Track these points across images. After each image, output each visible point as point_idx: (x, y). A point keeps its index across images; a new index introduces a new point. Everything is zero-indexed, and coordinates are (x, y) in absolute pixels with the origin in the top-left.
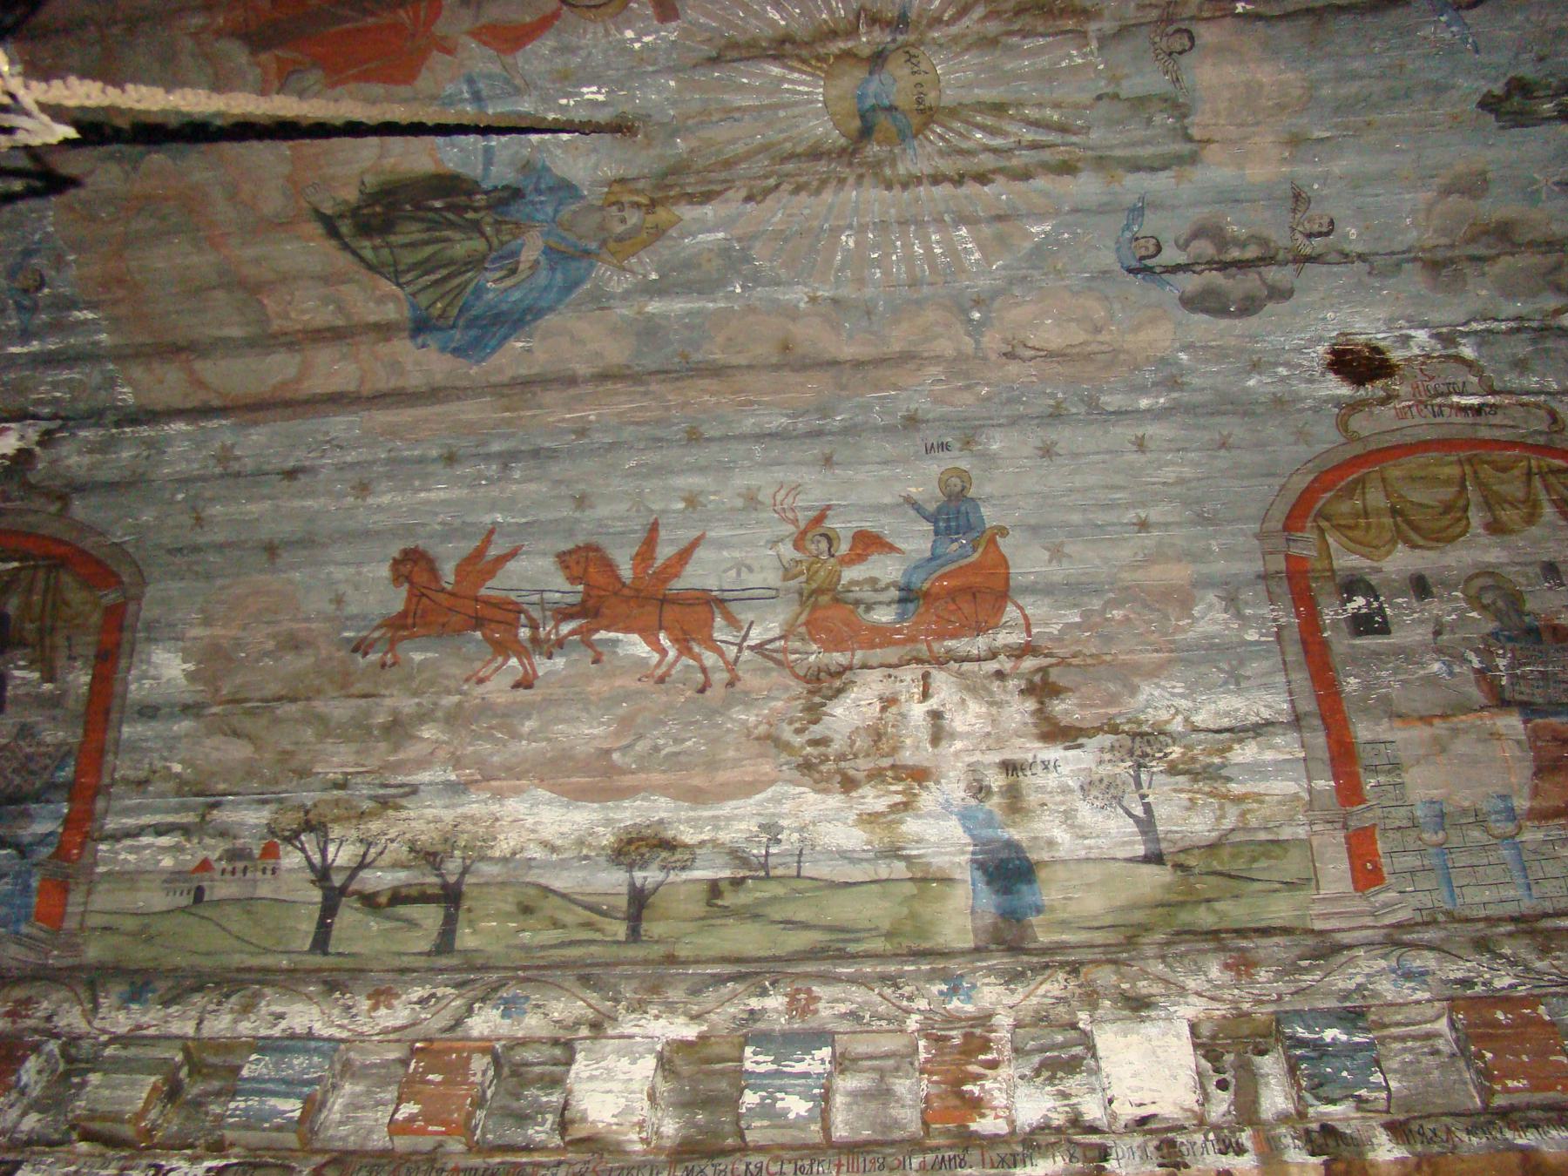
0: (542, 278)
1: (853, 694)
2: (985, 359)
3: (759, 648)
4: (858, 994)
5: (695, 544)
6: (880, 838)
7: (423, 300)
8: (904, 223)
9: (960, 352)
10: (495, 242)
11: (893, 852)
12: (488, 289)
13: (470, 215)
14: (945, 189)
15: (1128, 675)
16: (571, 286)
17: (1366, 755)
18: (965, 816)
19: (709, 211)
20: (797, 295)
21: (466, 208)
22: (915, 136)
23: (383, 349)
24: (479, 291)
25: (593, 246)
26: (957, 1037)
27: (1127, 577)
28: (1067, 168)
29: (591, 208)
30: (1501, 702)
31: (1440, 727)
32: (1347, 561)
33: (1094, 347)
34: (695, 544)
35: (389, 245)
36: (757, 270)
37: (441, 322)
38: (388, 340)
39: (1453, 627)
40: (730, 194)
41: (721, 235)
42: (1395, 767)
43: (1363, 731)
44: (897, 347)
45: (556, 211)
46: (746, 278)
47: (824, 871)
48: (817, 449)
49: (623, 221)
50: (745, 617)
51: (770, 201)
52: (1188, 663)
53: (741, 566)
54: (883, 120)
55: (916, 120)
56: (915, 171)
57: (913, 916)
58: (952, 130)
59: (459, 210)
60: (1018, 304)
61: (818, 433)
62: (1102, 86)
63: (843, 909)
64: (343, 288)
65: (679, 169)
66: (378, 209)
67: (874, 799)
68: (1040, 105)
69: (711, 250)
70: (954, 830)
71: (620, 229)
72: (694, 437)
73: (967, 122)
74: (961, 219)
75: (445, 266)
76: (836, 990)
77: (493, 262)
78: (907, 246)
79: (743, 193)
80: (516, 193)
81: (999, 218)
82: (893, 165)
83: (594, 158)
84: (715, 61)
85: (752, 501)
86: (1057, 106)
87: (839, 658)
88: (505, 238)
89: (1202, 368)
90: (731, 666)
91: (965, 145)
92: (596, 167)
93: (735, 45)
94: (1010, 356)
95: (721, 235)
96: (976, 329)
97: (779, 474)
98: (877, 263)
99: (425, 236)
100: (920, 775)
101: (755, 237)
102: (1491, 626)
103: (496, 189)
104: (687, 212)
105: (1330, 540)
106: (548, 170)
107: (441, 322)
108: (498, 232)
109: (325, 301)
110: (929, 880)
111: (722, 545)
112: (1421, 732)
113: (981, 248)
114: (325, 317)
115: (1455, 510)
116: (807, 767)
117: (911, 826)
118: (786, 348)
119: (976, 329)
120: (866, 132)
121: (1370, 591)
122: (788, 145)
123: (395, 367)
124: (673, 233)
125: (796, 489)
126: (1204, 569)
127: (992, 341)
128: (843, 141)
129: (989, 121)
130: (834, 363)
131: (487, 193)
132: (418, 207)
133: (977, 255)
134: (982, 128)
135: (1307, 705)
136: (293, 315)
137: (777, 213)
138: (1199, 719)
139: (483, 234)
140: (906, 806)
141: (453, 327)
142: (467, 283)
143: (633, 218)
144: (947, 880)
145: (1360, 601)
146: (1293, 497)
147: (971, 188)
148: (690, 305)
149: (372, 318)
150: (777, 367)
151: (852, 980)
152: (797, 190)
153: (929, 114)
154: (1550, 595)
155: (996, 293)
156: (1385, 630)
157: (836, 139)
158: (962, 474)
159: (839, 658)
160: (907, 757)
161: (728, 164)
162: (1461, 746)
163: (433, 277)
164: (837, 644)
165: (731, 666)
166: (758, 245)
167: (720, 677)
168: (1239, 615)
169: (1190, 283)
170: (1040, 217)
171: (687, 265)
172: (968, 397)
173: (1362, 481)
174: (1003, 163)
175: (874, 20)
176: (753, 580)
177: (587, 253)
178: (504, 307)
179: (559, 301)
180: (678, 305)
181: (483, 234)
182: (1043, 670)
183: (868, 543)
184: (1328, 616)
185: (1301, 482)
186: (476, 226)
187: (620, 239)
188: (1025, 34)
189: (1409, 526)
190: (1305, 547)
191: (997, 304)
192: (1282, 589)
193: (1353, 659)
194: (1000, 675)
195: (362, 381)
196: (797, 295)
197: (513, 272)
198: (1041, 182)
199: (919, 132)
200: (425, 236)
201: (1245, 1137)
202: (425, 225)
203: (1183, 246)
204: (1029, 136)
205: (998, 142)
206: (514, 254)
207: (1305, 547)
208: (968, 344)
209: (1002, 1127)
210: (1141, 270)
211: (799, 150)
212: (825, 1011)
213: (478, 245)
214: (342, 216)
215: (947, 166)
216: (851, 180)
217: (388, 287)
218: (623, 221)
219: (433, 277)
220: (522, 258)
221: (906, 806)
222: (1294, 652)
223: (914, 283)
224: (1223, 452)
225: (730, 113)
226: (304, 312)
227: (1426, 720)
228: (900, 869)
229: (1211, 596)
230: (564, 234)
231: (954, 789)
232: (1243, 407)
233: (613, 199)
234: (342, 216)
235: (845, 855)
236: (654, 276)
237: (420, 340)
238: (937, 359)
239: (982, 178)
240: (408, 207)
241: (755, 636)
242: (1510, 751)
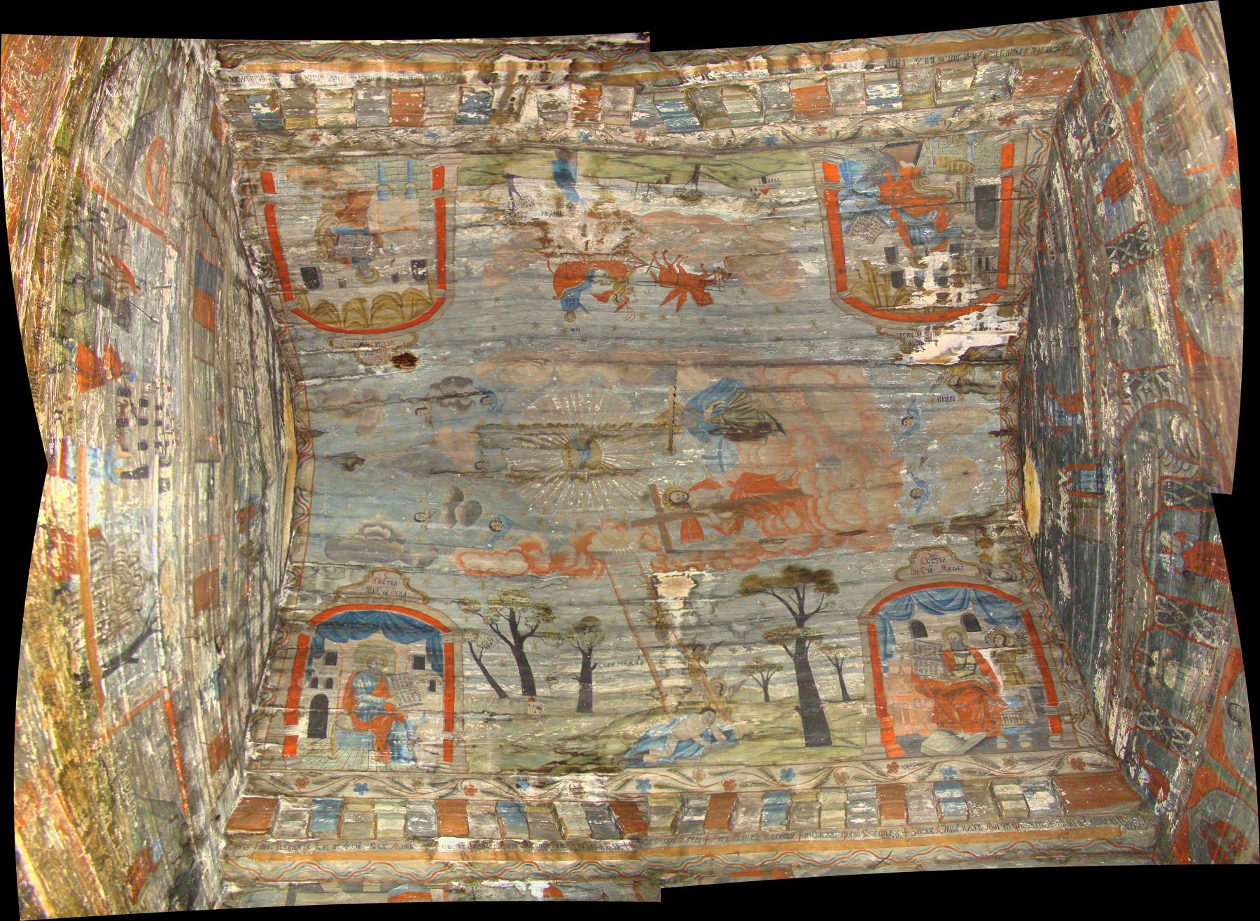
0: (705, 402)
8: (578, 412)
14: (563, 422)
16: (695, 399)
19: (645, 421)
24: (727, 400)
28: (522, 427)
30: (375, 236)
53: (648, 294)
54: (582, 446)
62: (507, 452)
65: (654, 436)
74: (558, 412)
80: (711, 433)
84: (638, 470)
93: (631, 475)
96: (555, 374)
101: (630, 411)
104: (652, 421)
119: (555, 374)
120: (588, 443)
126: (477, 284)
137: (622, 419)
145: (420, 273)
153: (567, 447)
156: (413, 262)
157: (599, 442)
161: (636, 436)
171: (653, 403)
175: (582, 479)
184: (434, 267)
186: (727, 422)
188: (532, 471)
192: (448, 277)
198: (530, 423)
204: (533, 438)
213: (727, 417)
215: (563, 430)
225: (634, 452)
239: (550, 425)
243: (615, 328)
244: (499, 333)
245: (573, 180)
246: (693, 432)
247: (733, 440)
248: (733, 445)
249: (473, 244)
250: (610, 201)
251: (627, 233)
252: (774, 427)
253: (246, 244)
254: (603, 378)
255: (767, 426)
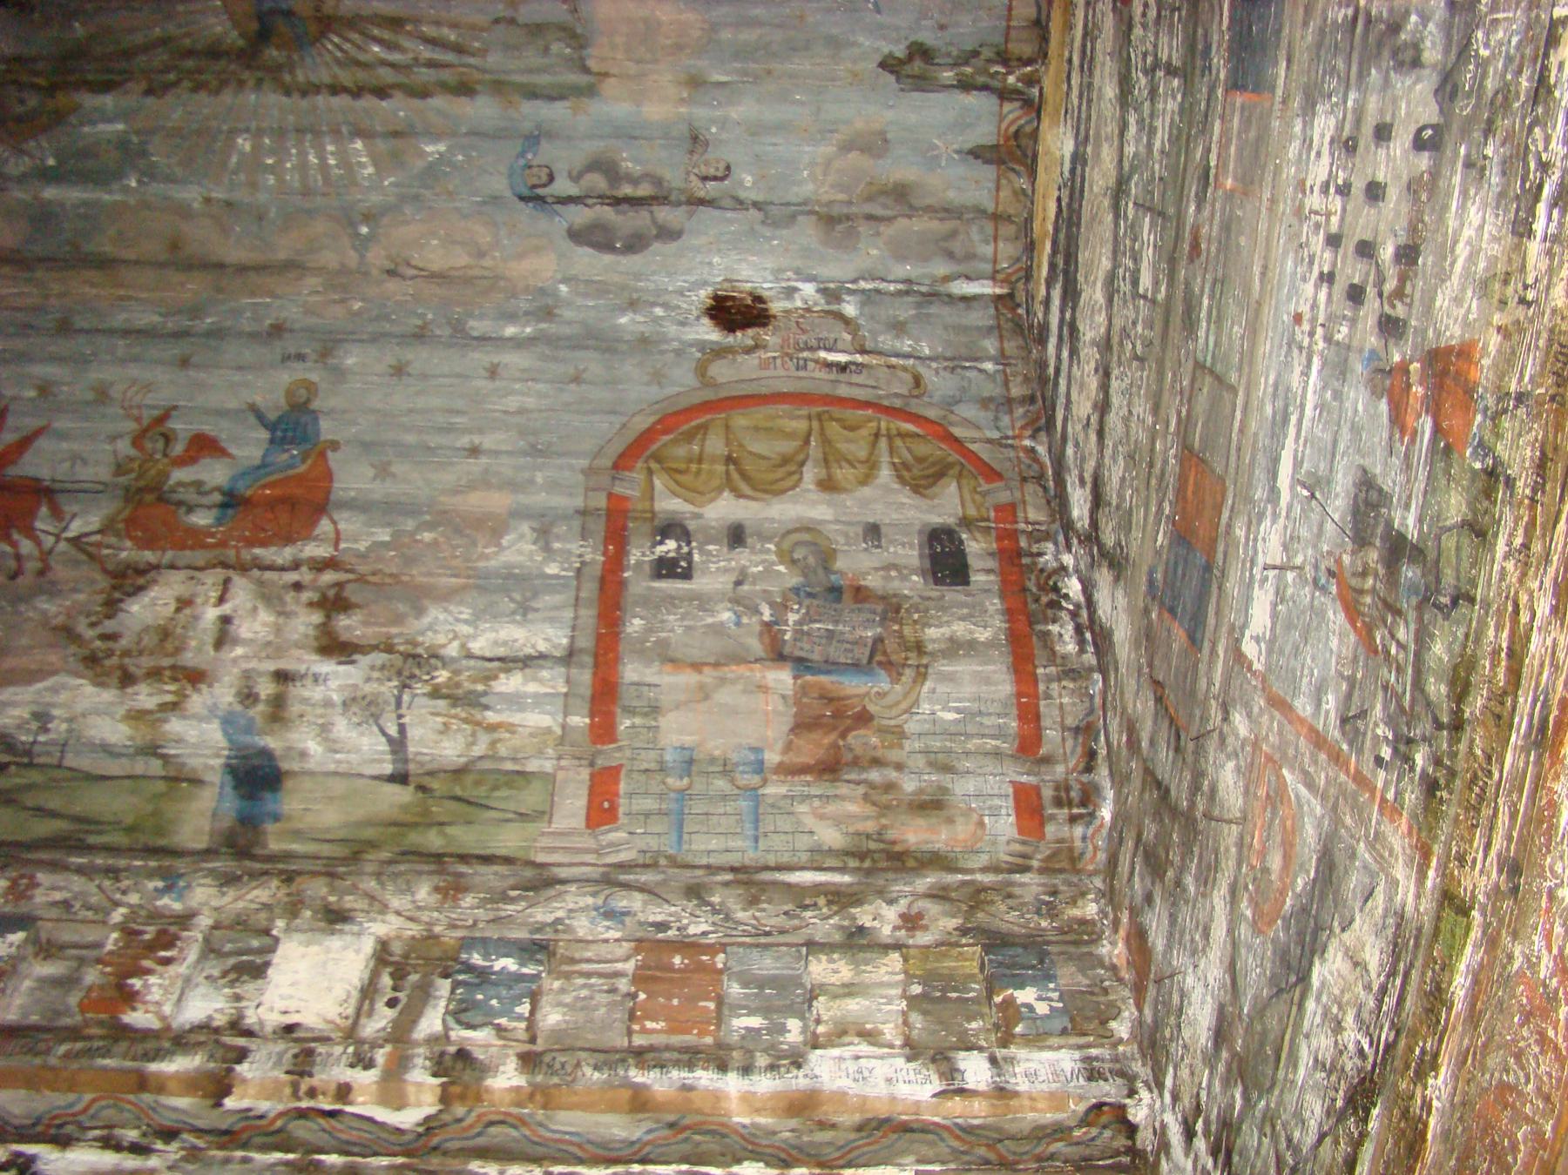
1: (154, 592)
2: (366, 274)
3: (76, 541)
4: (78, 883)
5: (39, 432)
6: (143, 735)
8: (300, 131)
9: (343, 265)
11: (152, 750)
14: (343, 101)
15: (419, 598)
17: (627, 696)
18: (228, 721)
19: (108, 101)
20: (191, 194)
22: (312, 44)
26: (150, 933)
27: (447, 501)
28: (464, 89)
30: (778, 655)
31: (709, 675)
32: (670, 504)
33: (477, 272)
34: (39, 432)
36: (153, 165)
39: (756, 578)
41: (120, 127)
42: (654, 710)
43: (631, 671)
44: (282, 255)
47: (85, 763)
48: (175, 350)
49: (22, 102)
50: (69, 509)
51: (169, 98)
52: (482, 589)
54: (281, 25)
55: (313, 28)
56: (314, 79)
57: (156, 813)
58: (347, 40)
60: (407, 223)
61: (179, 335)
63: (97, 802)
67: (146, 697)
68: (438, 23)
70: (213, 733)
72: (65, 328)
73: (362, 33)
74: (358, 133)
76: (58, 879)
78: (303, 154)
79: (144, 85)
81: (396, 134)
82: (292, 72)
85: (102, 395)
86: (454, 26)
87: (149, 556)
89: (580, 301)
90: (45, 555)
91: (362, 57)
94: (391, 273)
95: (120, 127)
97: (134, 371)
98: (271, 169)
100: (196, 677)
101: (152, 132)
102: (795, 580)
104: (89, 101)
105: (657, 483)
110: (181, 779)
111: (63, 436)
112: (688, 678)
113: (376, 165)
115: (791, 465)
116: (92, 660)
117: (175, 726)
118: (175, 246)
119: (362, 244)
120: (264, 35)
121: (685, 535)
122: (187, 42)
124: (73, 120)
125: (148, 387)
126: (523, 499)
127: (377, 257)
128: (241, 43)
129: (386, 35)
130: (221, 266)
133: (370, 170)
134: (380, 41)
135: (586, 642)
138: (476, 646)
140: (174, 706)
143: (33, 101)
144: (196, 782)
145: (671, 545)
146: (631, 436)
147: (368, 102)
150: (162, 265)
151: (80, 870)
152: (196, 89)
154: (862, 556)
155: (386, 210)
156: (687, 575)
157: (234, 38)
158: (311, 388)
159: (149, 556)
160: (189, 658)
161: (128, 54)
162: (724, 696)
164: (148, 543)
165: (45, 555)
166: (157, 139)
167: (32, 566)
168: (547, 549)
169: (580, 216)
170: (436, 137)
171: (85, 154)
172: (339, 311)
173: (704, 428)
174: (402, 79)
176: (86, 473)
180: (73, 195)
182: (340, 585)
183: (203, 446)
184: (635, 555)
185: (642, 423)
189: (741, 475)
190: (630, 487)
191: (385, 220)
192: (599, 526)
193: (645, 601)
194: (297, 586)
196: (191, 194)
199: (317, 40)
201: (381, 1056)
203: (576, 178)
204: (426, 53)
205: (396, 57)
207: (630, 487)
208: (352, 259)
209: (156, 1024)
210: (533, 198)
211: (199, 47)
212: (40, 897)
215: (346, 77)
216: (251, 83)
221: (174, 706)
222: (590, 589)
223: (306, 192)
224: (573, 386)
227: (697, 666)
228: (155, 767)
229: (525, 527)
231: (224, 693)
232: (603, 342)
235: (107, 749)
236: (51, 162)
238: (320, 270)
239: (382, 92)
241: (75, 528)
242: (773, 704)
243: (185, 363)
244: (481, 357)
245: (231, 769)
249: (525, 610)
250: (137, 716)
251: (109, 626)
253: (1090, 658)
254: (225, 231)
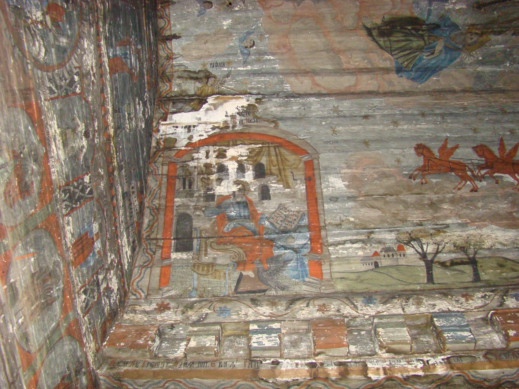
0: (443, 56)
7: (400, 61)
10: (427, 42)
12: (424, 59)
13: (420, 32)
16: (451, 61)
19: (500, 37)
21: (419, 30)
23: (386, 76)
24: (421, 59)
25: (461, 47)
29: (462, 34)
35: (390, 41)
36: (514, 59)
37: (406, 69)
38: (388, 74)
40: (508, 32)
45: (450, 34)
46: (511, 61)
59: (417, 30)
64: (371, 54)
66: (388, 27)
69: (500, 51)
71: (470, 41)
75: (410, 49)
77: (427, 49)
80: (437, 26)
83: (465, 17)
88: (431, 41)
92: (466, 19)
95: (503, 46)
99: (403, 38)
103: (430, 24)
104: (493, 37)
106: (450, 19)
107: (406, 69)
108: (429, 39)
109: (364, 59)
114: (364, 64)
123: (390, 83)
131: (427, 25)
132: (402, 28)
136: (351, 62)
139: (424, 40)
141: (411, 71)
142: (416, 56)
143: (475, 38)
148: (492, 69)
149: (381, 66)
163: (404, 53)
171: (493, 55)
177: (458, 49)
178: (429, 65)
179: (448, 65)
180: (488, 69)
181: (424, 40)
186: (422, 37)
187: (469, 45)
195: (379, 87)
197: (433, 53)
200: (403, 38)
202: (404, 35)
206: (434, 47)
213: (422, 43)
214: (374, 29)
217: (387, 55)
218: (471, 39)
219: (404, 53)
220: (436, 49)
226: (356, 62)
230: (451, 42)
233: (469, 31)
234: (374, 29)
236: (480, 58)
237: (400, 75)
240: (399, 28)
246: (454, 26)
247: (417, 19)
248: (416, 13)
252: (375, 33)
255: (382, 34)
